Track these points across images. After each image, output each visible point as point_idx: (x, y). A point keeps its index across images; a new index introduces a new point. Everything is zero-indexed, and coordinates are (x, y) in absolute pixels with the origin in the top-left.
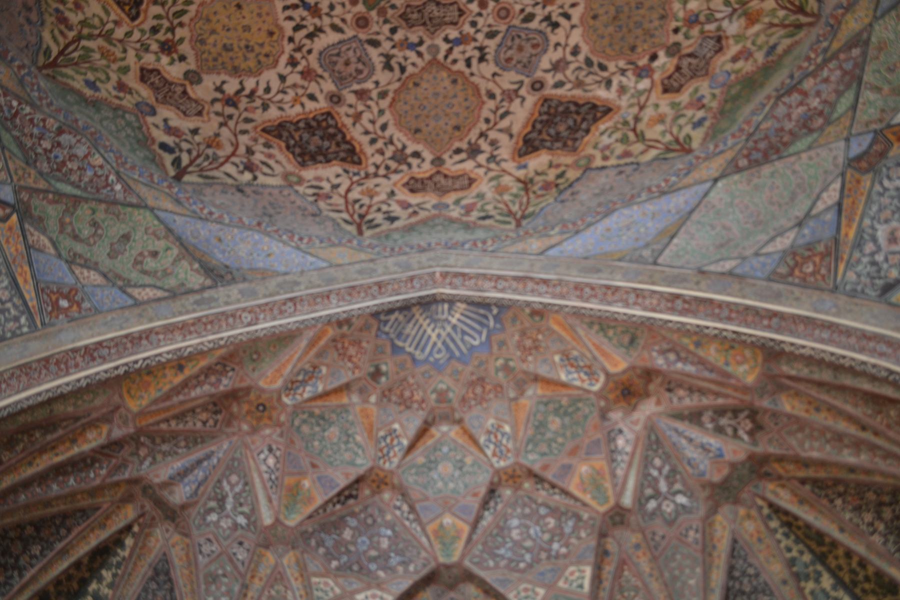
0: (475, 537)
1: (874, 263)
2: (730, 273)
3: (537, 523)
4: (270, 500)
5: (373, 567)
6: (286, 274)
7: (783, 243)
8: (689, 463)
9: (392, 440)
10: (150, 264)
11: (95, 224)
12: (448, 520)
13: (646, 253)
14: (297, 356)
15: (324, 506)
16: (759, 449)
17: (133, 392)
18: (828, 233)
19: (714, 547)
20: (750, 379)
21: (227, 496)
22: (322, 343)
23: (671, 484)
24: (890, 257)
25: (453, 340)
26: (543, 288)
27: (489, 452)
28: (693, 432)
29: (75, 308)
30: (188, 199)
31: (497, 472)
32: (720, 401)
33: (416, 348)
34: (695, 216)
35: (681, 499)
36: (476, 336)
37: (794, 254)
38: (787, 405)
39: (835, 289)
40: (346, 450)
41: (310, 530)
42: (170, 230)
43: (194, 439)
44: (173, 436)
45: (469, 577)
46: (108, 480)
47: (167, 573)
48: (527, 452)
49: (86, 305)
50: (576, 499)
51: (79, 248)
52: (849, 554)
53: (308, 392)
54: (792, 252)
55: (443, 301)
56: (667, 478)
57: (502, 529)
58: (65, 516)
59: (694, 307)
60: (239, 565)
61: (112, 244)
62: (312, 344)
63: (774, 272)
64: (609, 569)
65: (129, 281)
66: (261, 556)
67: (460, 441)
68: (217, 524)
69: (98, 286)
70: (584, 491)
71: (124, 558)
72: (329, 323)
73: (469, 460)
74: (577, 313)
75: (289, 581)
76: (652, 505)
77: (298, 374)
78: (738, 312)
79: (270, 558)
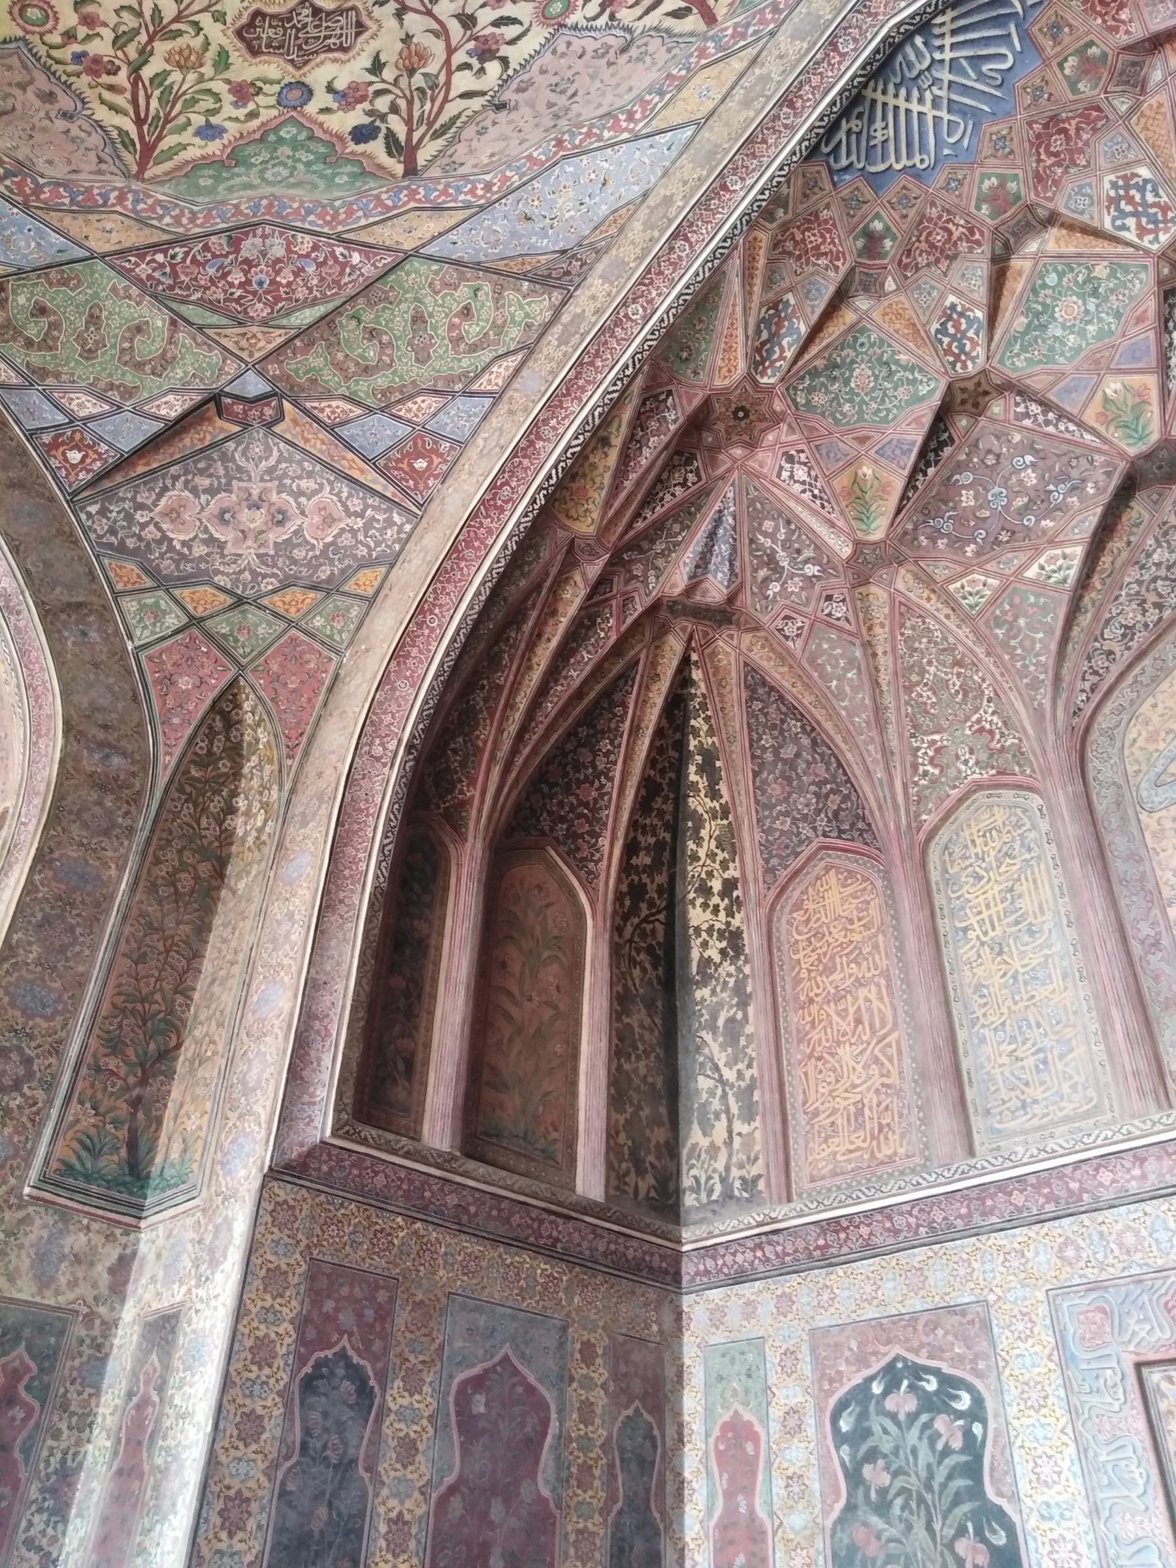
4: (832, 525)
5: (1030, 521)
6: (645, 195)
9: (957, 326)
10: (472, 330)
11: (372, 334)
14: (739, 309)
17: (573, 513)
21: (774, 552)
22: (761, 262)
25: (966, 90)
27: (1131, 236)
29: (436, 460)
30: (444, 192)
33: (909, 156)
36: (1003, 50)
40: (895, 389)
41: (910, 526)
42: (458, 263)
43: (687, 511)
44: (659, 526)
46: (624, 628)
47: (764, 683)
49: (445, 446)
51: (381, 381)
53: (788, 346)
55: (909, 37)
58: (607, 694)
65: (465, 374)
66: (864, 597)
67: (1071, 250)
71: (704, 695)
73: (1101, 271)
75: (919, 606)
77: (758, 332)
79: (878, 593)
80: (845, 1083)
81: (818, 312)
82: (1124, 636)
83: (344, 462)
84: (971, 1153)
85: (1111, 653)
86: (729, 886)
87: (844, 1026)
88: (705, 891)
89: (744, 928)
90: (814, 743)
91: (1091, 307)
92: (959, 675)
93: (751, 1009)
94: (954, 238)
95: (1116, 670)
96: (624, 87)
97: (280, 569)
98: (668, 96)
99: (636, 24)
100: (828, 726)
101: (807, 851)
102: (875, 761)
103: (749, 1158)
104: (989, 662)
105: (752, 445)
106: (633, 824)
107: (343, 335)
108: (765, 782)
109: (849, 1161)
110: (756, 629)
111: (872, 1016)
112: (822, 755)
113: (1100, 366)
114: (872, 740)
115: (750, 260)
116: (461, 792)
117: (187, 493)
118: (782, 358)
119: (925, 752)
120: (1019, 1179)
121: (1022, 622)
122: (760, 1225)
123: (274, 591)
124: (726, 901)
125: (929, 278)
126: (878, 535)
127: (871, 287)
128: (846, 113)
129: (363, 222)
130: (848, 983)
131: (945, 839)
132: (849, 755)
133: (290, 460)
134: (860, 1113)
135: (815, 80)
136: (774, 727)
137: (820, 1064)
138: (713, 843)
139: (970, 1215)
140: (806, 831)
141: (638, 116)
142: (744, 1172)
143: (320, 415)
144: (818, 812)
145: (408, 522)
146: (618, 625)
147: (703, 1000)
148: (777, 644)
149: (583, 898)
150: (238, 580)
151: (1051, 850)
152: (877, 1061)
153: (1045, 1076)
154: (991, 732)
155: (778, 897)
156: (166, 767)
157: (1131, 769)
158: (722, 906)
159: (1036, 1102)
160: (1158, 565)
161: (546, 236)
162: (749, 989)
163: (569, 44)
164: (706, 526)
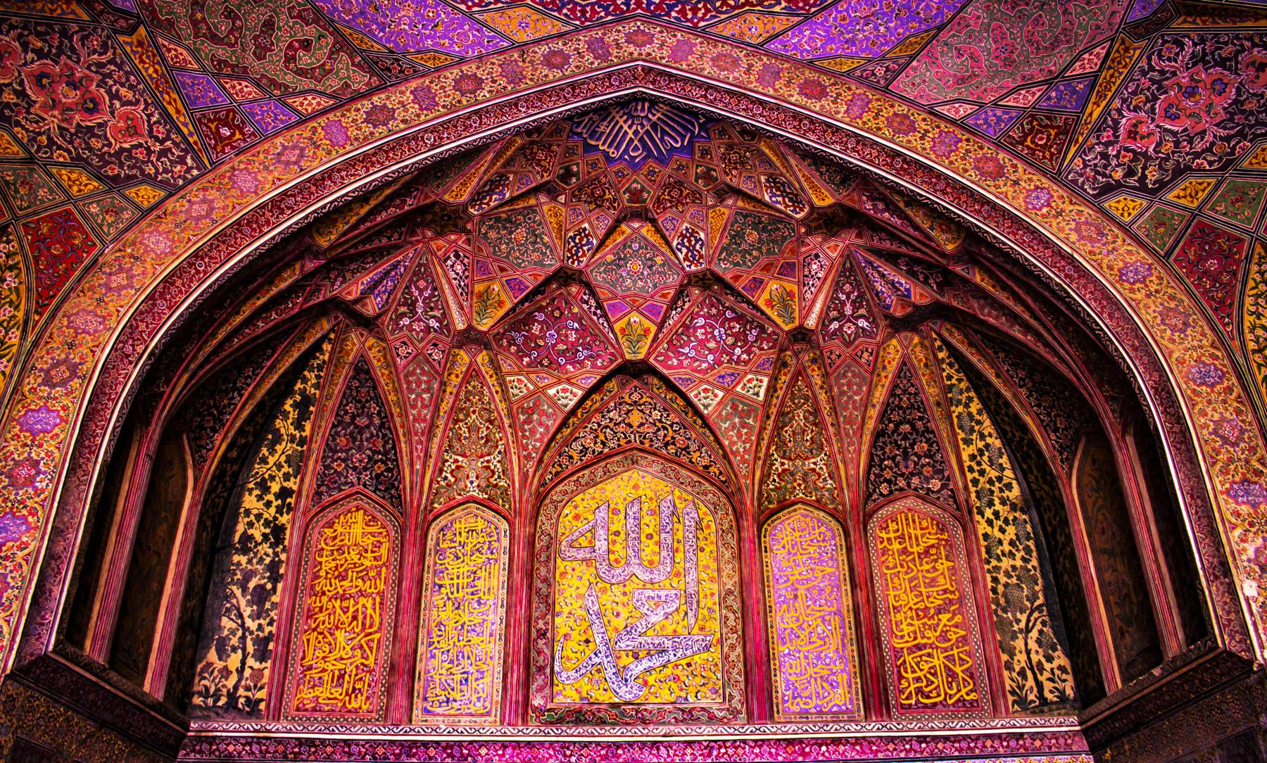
0: (661, 336)
1: (1104, 156)
2: (960, 124)
3: (722, 325)
4: (461, 307)
5: (562, 361)
6: (462, 61)
7: (1026, 99)
8: (877, 294)
9: (581, 240)
10: (304, 59)
13: (880, 71)
15: (513, 309)
16: (945, 300)
19: (884, 368)
20: (950, 247)
22: (509, 153)
23: (855, 309)
26: (758, 110)
27: (681, 257)
29: (238, 136)
32: (918, 254)
33: (609, 147)
34: (943, 36)
35: (862, 323)
44: (362, 255)
45: (655, 373)
47: (368, 372)
50: (763, 313)
51: (222, 52)
52: (998, 394)
53: (494, 200)
55: (644, 100)
56: (853, 303)
57: (688, 328)
60: (436, 364)
61: (256, 38)
63: (1006, 134)
64: (784, 379)
65: (287, 87)
67: (652, 240)
68: (410, 328)
69: (256, 100)
70: (772, 307)
72: (518, 134)
73: (659, 260)
74: (791, 144)
76: (835, 325)
77: (485, 185)
78: (953, 188)
79: (464, 357)
80: (336, 654)
83: (166, 96)
84: (410, 721)
85: (571, 457)
86: (284, 493)
87: (344, 618)
88: (264, 488)
89: (289, 526)
90: (382, 425)
92: (488, 428)
93: (280, 586)
97: (76, 149)
100: (398, 421)
101: (347, 490)
102: (418, 456)
103: (255, 686)
105: (440, 234)
106: (241, 430)
108: (337, 434)
110: (382, 340)
111: (365, 618)
112: (384, 435)
114: (421, 443)
116: (158, 387)
117: (17, 44)
118: (487, 204)
119: (450, 466)
120: (437, 743)
121: (535, 417)
122: (255, 731)
123: (63, 165)
124: (279, 502)
125: (583, 207)
126: (484, 329)
127: (554, 197)
130: (354, 591)
131: (444, 523)
132: (403, 445)
133: (120, 67)
134: (341, 676)
136: (360, 401)
137: (320, 637)
138: (283, 458)
139: (400, 754)
140: (353, 478)
142: (250, 694)
145: (198, 168)
147: (239, 564)
149: (190, 474)
150: (34, 139)
152: (361, 647)
153: (464, 688)
155: (317, 514)
157: (560, 531)
158: (275, 504)
159: (455, 700)
160: (611, 420)
161: (383, 30)
162: (282, 571)
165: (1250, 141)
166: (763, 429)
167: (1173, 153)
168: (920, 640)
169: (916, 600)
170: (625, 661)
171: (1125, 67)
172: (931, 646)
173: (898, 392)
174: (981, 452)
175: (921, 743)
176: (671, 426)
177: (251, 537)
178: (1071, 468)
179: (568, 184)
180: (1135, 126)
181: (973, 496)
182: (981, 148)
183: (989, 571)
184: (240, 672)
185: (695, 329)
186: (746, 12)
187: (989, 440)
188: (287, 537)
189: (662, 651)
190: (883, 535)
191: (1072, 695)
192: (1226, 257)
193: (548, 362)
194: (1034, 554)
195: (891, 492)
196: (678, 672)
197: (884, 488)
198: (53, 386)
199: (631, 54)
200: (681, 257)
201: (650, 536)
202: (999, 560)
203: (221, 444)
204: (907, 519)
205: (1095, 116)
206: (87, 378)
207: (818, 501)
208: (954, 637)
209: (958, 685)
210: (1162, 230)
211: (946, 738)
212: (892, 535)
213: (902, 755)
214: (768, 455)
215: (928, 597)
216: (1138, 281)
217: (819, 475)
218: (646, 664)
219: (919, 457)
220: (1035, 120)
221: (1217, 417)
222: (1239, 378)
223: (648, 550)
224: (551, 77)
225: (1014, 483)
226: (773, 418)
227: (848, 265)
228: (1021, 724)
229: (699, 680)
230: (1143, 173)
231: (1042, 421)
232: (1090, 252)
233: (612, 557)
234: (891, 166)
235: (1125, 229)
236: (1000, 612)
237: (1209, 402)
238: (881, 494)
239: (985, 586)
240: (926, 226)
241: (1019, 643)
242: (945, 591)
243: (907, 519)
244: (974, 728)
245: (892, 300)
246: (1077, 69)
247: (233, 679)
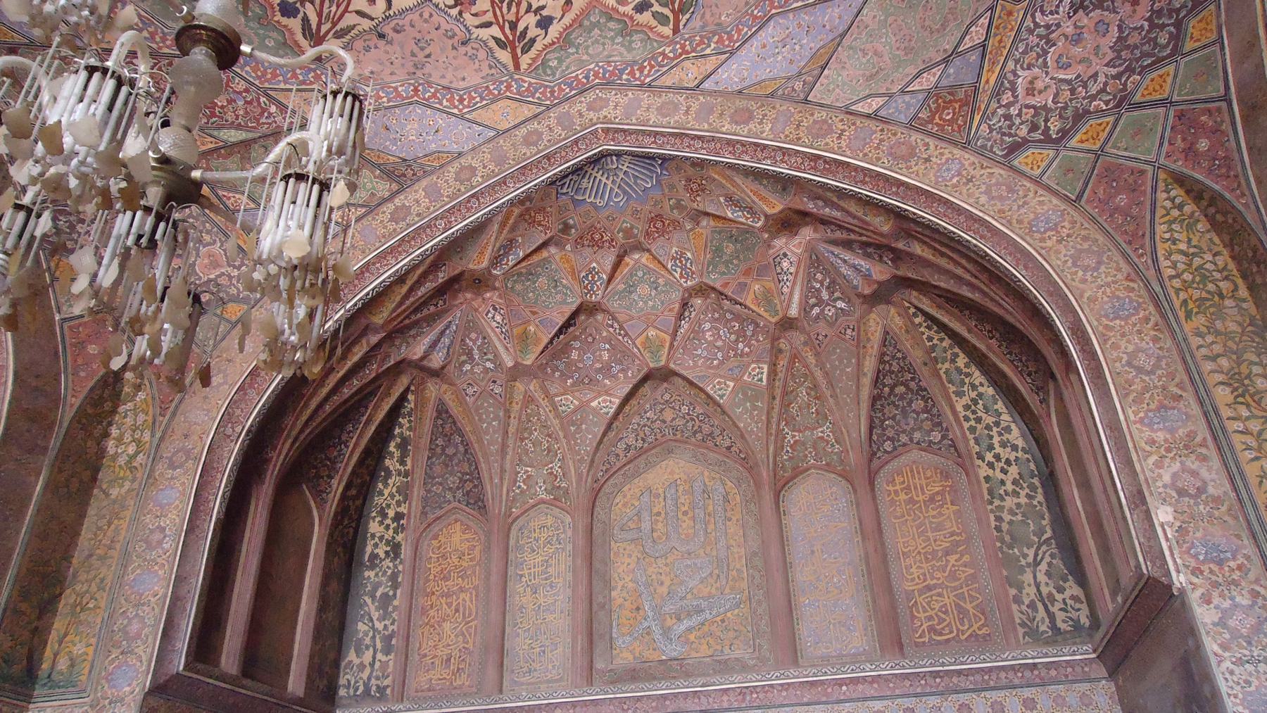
1: (1007, 117)
4: (507, 348)
5: (599, 377)
7: (928, 80)
9: (593, 277)
12: (652, 333)
13: (798, 85)
15: (551, 342)
16: (899, 273)
18: (969, 79)
19: (869, 340)
20: (886, 228)
22: (511, 222)
24: (1024, 110)
25: (627, 184)
26: (698, 144)
27: (677, 276)
28: (847, 256)
31: (686, 290)
32: (864, 239)
34: (847, 41)
35: (840, 304)
37: (938, 96)
38: (918, 249)
39: (965, 146)
40: (556, 294)
43: (431, 320)
44: (417, 323)
47: (447, 412)
48: (708, 273)
54: (933, 93)
56: (828, 288)
57: (697, 333)
58: (360, 401)
59: (833, 168)
62: (503, 225)
63: (915, 117)
64: (783, 363)
67: (651, 266)
74: (731, 167)
76: (816, 310)
77: (499, 250)
78: (871, 177)
79: (520, 386)
81: (531, 249)
82: (626, 449)
84: (501, 691)
85: (618, 455)
86: (398, 516)
89: (403, 543)
90: (466, 451)
91: (653, 294)
93: (399, 592)
94: (605, 239)
95: (618, 465)
96: (460, 74)
98: (485, 102)
99: (474, 30)
104: (564, 441)
106: (353, 472)
107: (254, 154)
108: (433, 463)
109: (438, 685)
111: (465, 609)
112: (469, 459)
113: (650, 324)
115: (507, 218)
119: (522, 476)
121: (584, 426)
125: (588, 251)
126: (528, 363)
127: (560, 245)
128: (573, 173)
129: (282, 86)
131: (521, 524)
132: (483, 465)
134: (449, 660)
135: (563, 154)
136: (446, 435)
138: (394, 490)
140: (449, 496)
141: (466, 103)
142: (379, 682)
143: (227, 202)
144: (458, 488)
146: (378, 369)
148: (460, 398)
149: (315, 513)
151: (569, 547)
152: (463, 634)
154: (556, 477)
156: (72, 405)
158: (392, 526)
159: (535, 670)
160: (648, 419)
162: (400, 580)
163: (431, 15)
164: (440, 327)
165: (1139, 74)
166: (770, 409)
167: (1071, 100)
168: (929, 582)
169: (924, 545)
170: (669, 622)
171: (1012, 30)
172: (940, 586)
173: (887, 358)
174: (975, 402)
175: (935, 678)
176: (698, 417)
177: (377, 556)
178: (1049, 407)
179: (568, 235)
180: (1031, 82)
181: (972, 442)
182: (895, 134)
183: (992, 511)
184: (372, 665)
185: (704, 332)
186: (683, 60)
187: (981, 389)
188: (403, 551)
189: (699, 611)
190: (890, 488)
191: (1087, 624)
192: (1134, 190)
193: (588, 381)
194: (1040, 490)
195: (895, 449)
196: (713, 628)
197: (888, 446)
198: (175, 469)
199: (591, 120)
200: (677, 276)
201: (685, 513)
202: (1002, 499)
203: (337, 486)
204: (912, 471)
205: (992, 81)
206: (197, 459)
207: (827, 464)
208: (963, 576)
209: (970, 621)
210: (1070, 175)
211: (959, 672)
212: (898, 487)
213: (919, 690)
214: (779, 431)
215: (935, 541)
216: (1050, 229)
217: (828, 442)
218: (686, 623)
219: (918, 414)
220: (939, 98)
221: (1131, 348)
222: (1158, 305)
223: (684, 525)
224: (528, 154)
225: (1013, 426)
226: (778, 399)
227: (814, 257)
228: (1032, 656)
229: (732, 634)
230: (1046, 126)
231: (1017, 367)
232: (999, 211)
233: (655, 535)
234: (814, 168)
235: (1037, 182)
236: (1005, 549)
237: (1123, 335)
238: (886, 452)
239: (989, 525)
240: (860, 214)
241: (1028, 577)
242: (952, 534)
243: (912, 471)
244: (984, 661)
245: (857, 281)
246: (967, 43)
247: (367, 671)
